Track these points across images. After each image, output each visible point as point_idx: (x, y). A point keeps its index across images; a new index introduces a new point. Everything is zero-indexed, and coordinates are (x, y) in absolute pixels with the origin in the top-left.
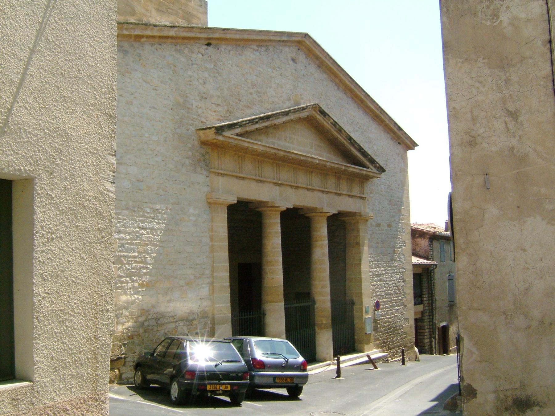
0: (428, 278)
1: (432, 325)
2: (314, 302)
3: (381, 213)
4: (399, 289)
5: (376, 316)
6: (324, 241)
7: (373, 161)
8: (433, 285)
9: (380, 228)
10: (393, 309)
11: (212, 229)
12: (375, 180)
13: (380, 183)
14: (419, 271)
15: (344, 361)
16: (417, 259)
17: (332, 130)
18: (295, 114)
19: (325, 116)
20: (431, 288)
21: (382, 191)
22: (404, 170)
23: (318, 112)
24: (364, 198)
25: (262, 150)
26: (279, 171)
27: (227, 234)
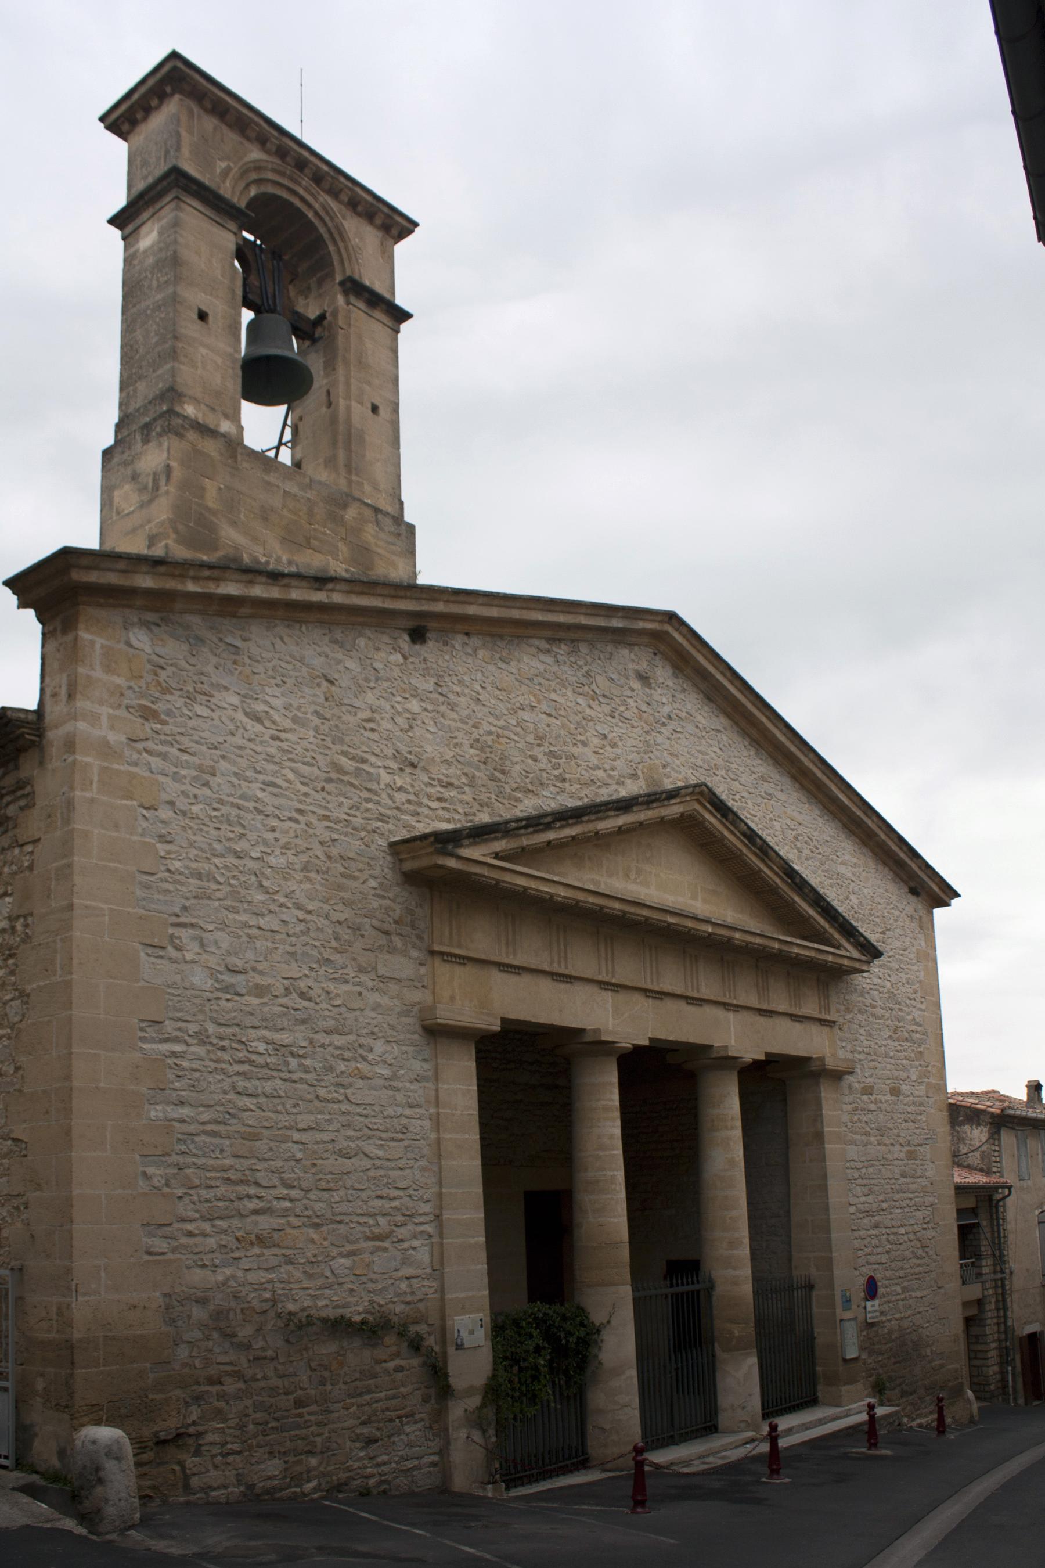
0: (992, 1219)
1: (1005, 1332)
2: (711, 1287)
3: (873, 1060)
4: (923, 1247)
5: (869, 1315)
6: (732, 1128)
7: (849, 931)
8: (1005, 1237)
9: (873, 1098)
10: (911, 1297)
11: (437, 1097)
12: (859, 980)
13: (868, 987)
14: (970, 1203)
15: (789, 1431)
16: (965, 1173)
17: (745, 850)
18: (648, 809)
19: (725, 816)
20: (1000, 1243)
21: (874, 1007)
22: (929, 958)
23: (708, 806)
24: (829, 1021)
25: (565, 897)
26: (613, 954)
27: (476, 1113)
